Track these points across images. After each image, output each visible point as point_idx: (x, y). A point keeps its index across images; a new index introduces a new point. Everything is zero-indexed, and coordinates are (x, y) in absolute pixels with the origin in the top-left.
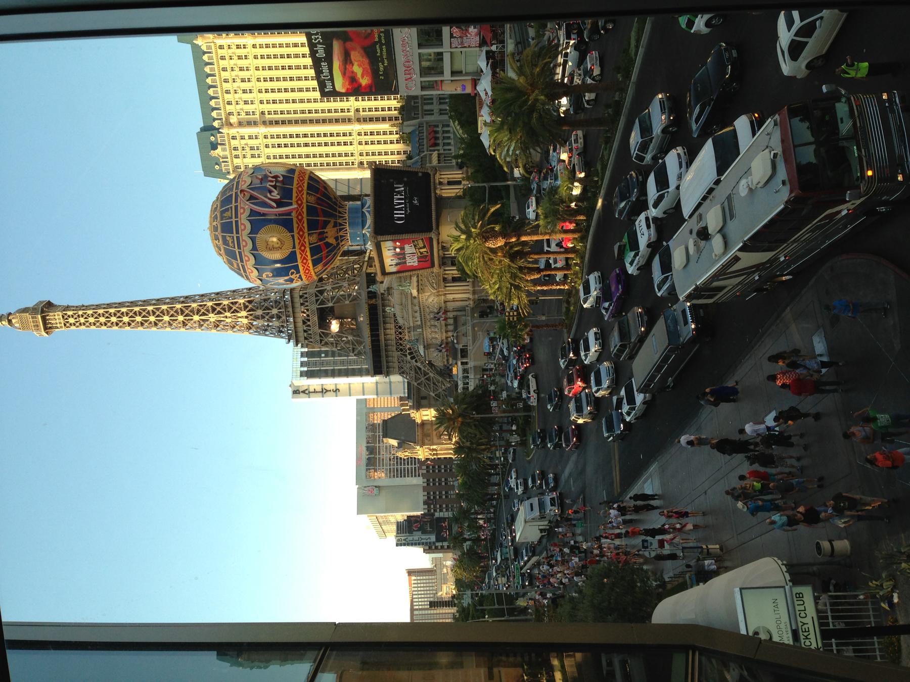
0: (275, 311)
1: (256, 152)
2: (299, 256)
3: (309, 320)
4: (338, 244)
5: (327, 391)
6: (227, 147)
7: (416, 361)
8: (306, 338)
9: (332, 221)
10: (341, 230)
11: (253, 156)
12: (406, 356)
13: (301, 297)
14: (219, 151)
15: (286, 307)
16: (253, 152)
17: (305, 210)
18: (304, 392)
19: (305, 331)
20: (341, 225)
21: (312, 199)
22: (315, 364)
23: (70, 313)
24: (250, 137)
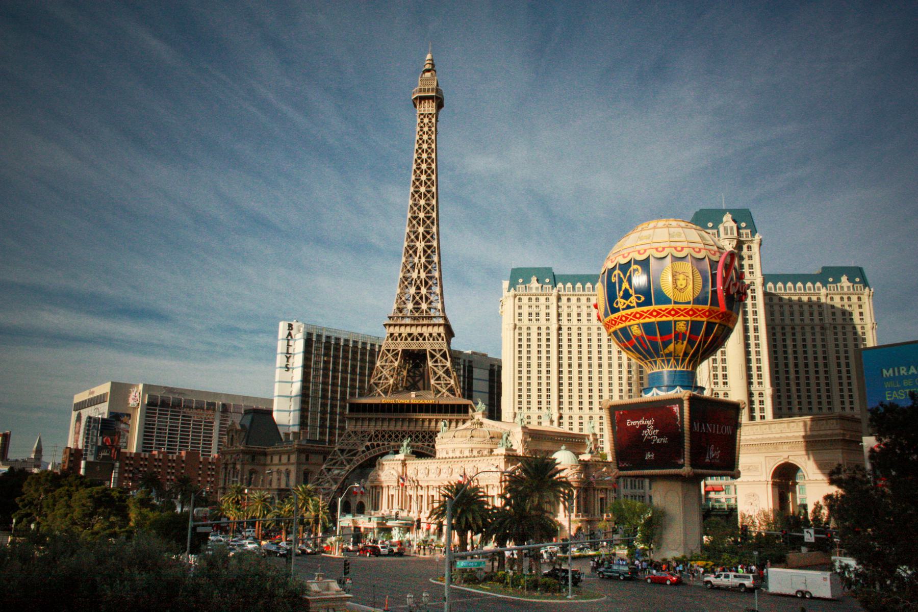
0: (424, 306)
1: (534, 317)
2: (663, 307)
3: (412, 340)
5: (288, 358)
6: (540, 292)
7: (363, 452)
8: (392, 334)
11: (530, 314)
13: (439, 335)
14: (534, 284)
16: (534, 315)
18: (290, 334)
19: (400, 335)
22: (317, 349)
23: (434, 120)
24: (548, 314)
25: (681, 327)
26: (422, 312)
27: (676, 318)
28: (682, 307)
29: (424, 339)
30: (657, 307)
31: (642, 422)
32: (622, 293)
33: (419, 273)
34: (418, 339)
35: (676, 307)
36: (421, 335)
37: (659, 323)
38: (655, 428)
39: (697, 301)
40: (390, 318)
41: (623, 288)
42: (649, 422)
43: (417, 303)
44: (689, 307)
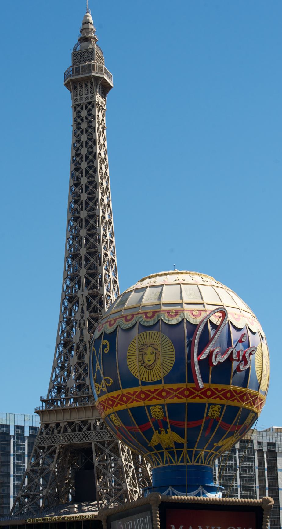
2: (132, 390)
3: (74, 430)
4: (150, 449)
9: (184, 441)
10: (172, 453)
17: (198, 400)
19: (58, 425)
20: (179, 453)
21: (214, 412)
22: (18, 447)
25: (157, 413)
28: (152, 388)
29: (89, 429)
30: (125, 391)
34: (81, 429)
36: (85, 422)
37: (131, 409)
39: (168, 379)
44: (160, 387)
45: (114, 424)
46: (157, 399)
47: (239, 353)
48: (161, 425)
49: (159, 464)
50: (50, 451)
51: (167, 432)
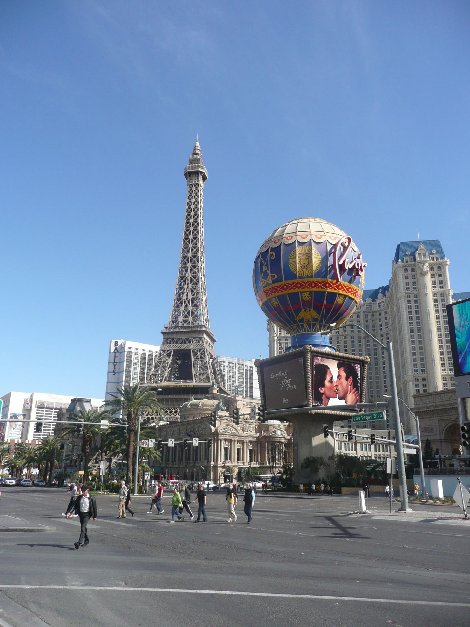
0: (190, 318)
2: (291, 281)
4: (295, 322)
9: (319, 317)
10: (309, 325)
12: (147, 415)
15: (194, 327)
19: (173, 340)
20: (314, 325)
22: (136, 358)
26: (189, 323)
27: (301, 290)
28: (306, 280)
29: (190, 342)
31: (280, 374)
32: (263, 274)
33: (187, 295)
35: (300, 280)
36: (188, 339)
37: (288, 294)
38: (288, 378)
40: (166, 328)
41: (264, 270)
42: (284, 374)
43: (186, 317)
45: (272, 304)
46: (308, 288)
47: (358, 264)
48: (307, 305)
49: (299, 332)
50: (168, 352)
51: (310, 310)
